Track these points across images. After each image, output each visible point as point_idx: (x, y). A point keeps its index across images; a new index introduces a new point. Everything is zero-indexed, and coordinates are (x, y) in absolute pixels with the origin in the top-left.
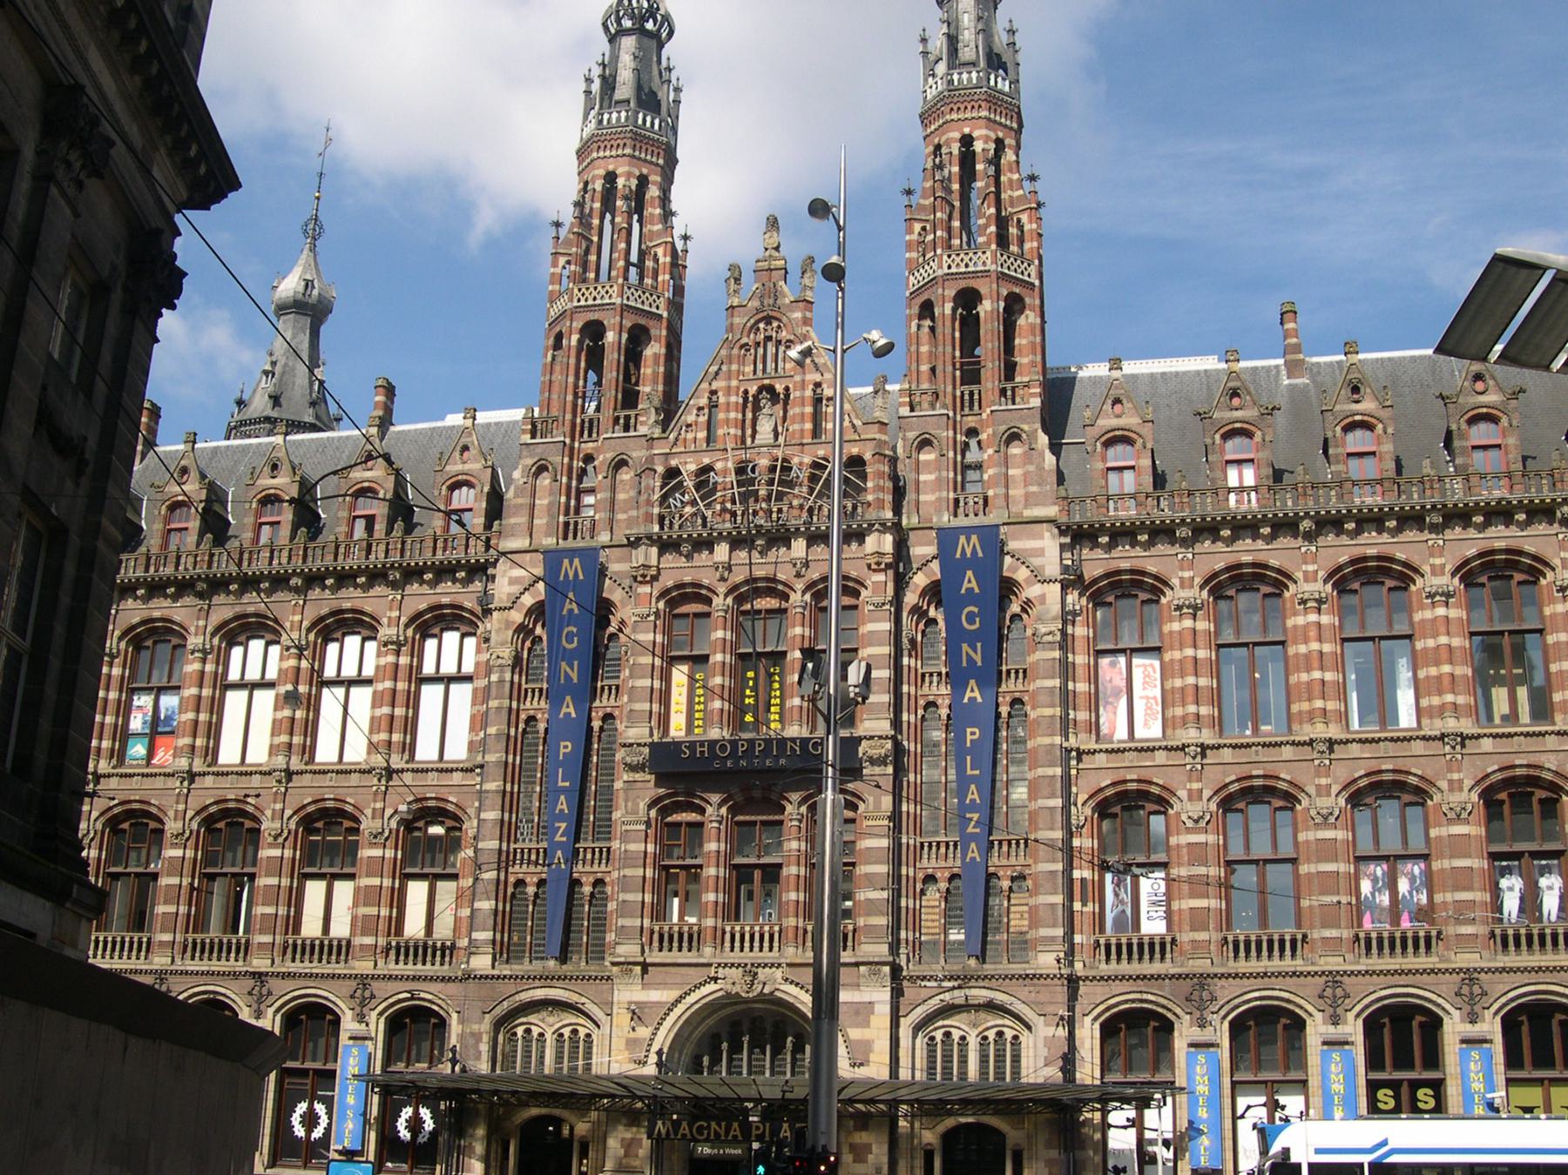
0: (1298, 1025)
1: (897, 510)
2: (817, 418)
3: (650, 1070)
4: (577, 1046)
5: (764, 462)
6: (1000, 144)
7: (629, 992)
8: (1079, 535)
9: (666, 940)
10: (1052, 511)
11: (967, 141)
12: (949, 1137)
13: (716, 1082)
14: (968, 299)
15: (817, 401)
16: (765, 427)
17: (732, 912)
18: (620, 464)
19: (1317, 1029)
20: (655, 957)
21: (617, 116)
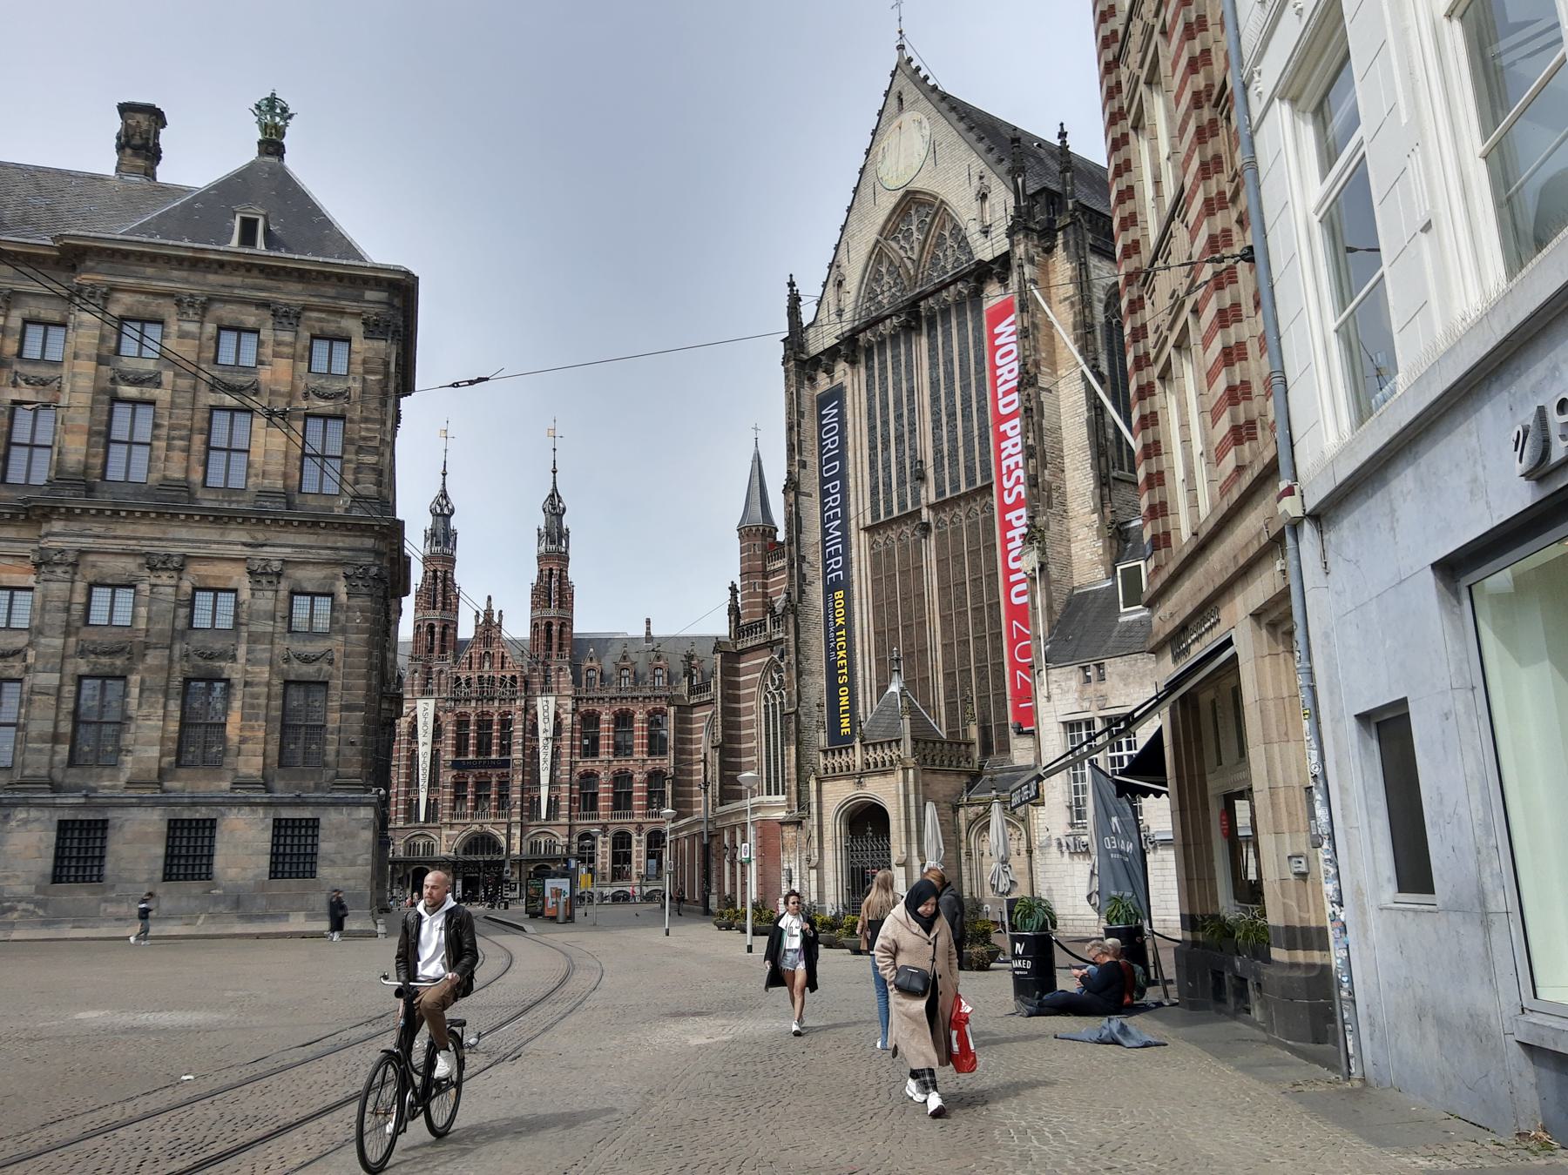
0: (630, 837)
1: (526, 692)
2: (503, 663)
3: (452, 854)
4: (429, 848)
5: (486, 676)
6: (561, 570)
7: (445, 832)
8: (577, 700)
9: (457, 816)
10: (570, 693)
11: (551, 570)
12: (536, 869)
13: (472, 858)
14: (549, 625)
15: (503, 657)
16: (487, 665)
17: (476, 808)
18: (441, 672)
19: (635, 837)
20: (454, 821)
21: (435, 549)
